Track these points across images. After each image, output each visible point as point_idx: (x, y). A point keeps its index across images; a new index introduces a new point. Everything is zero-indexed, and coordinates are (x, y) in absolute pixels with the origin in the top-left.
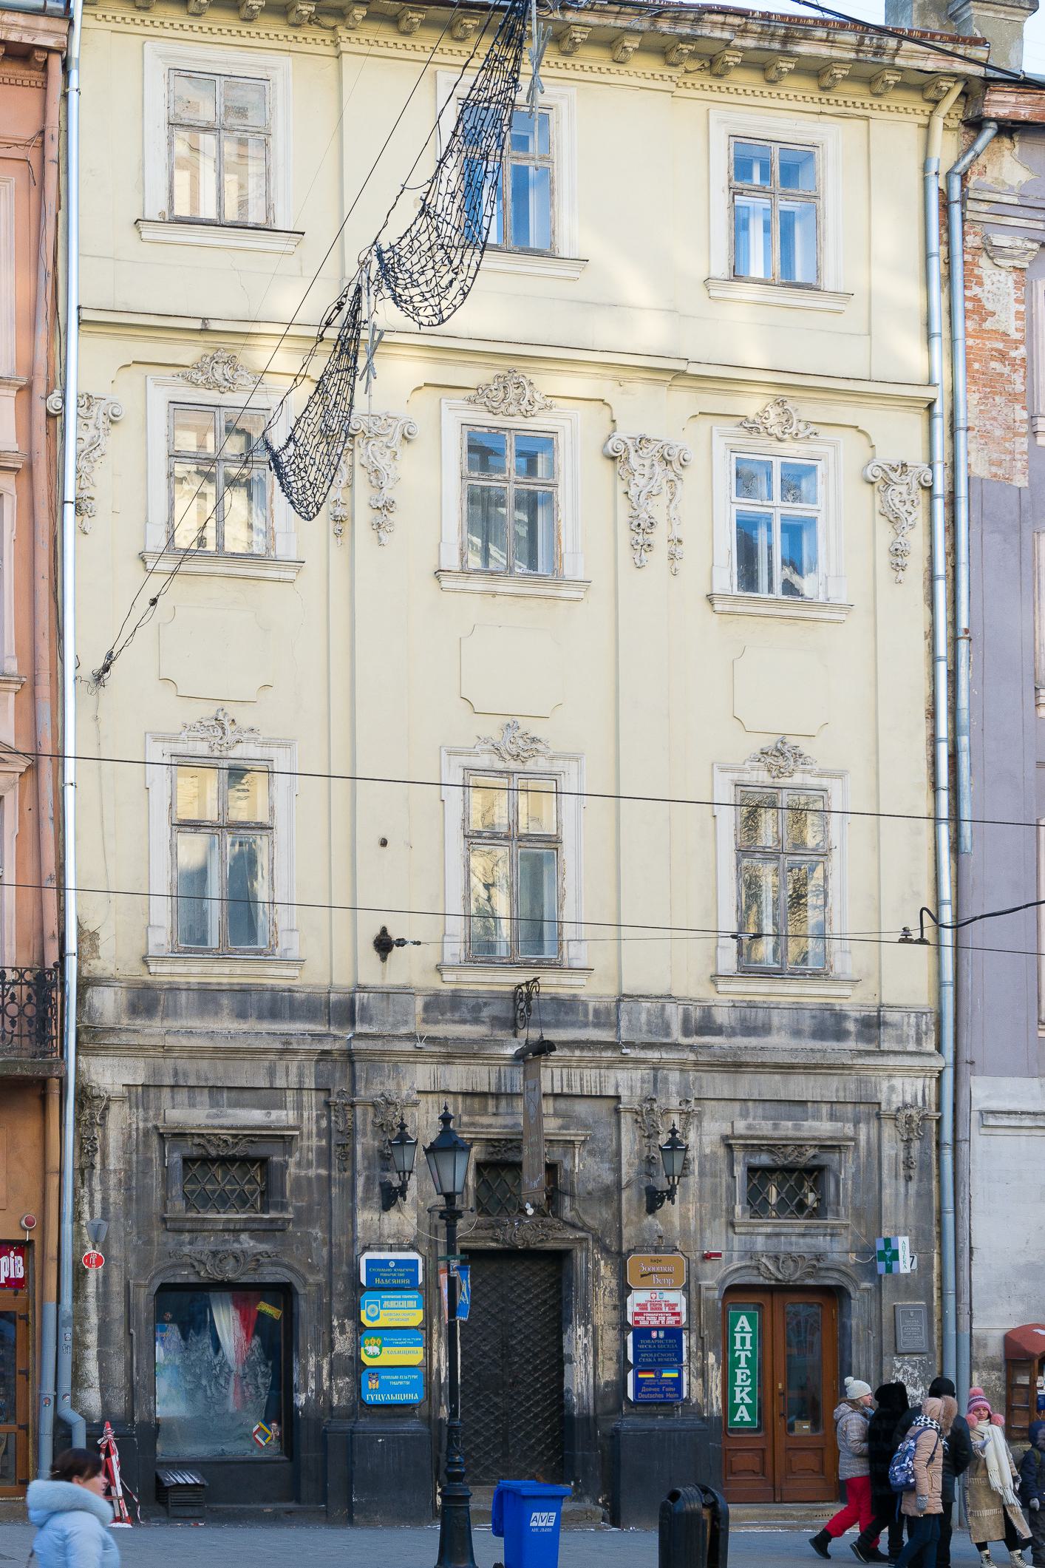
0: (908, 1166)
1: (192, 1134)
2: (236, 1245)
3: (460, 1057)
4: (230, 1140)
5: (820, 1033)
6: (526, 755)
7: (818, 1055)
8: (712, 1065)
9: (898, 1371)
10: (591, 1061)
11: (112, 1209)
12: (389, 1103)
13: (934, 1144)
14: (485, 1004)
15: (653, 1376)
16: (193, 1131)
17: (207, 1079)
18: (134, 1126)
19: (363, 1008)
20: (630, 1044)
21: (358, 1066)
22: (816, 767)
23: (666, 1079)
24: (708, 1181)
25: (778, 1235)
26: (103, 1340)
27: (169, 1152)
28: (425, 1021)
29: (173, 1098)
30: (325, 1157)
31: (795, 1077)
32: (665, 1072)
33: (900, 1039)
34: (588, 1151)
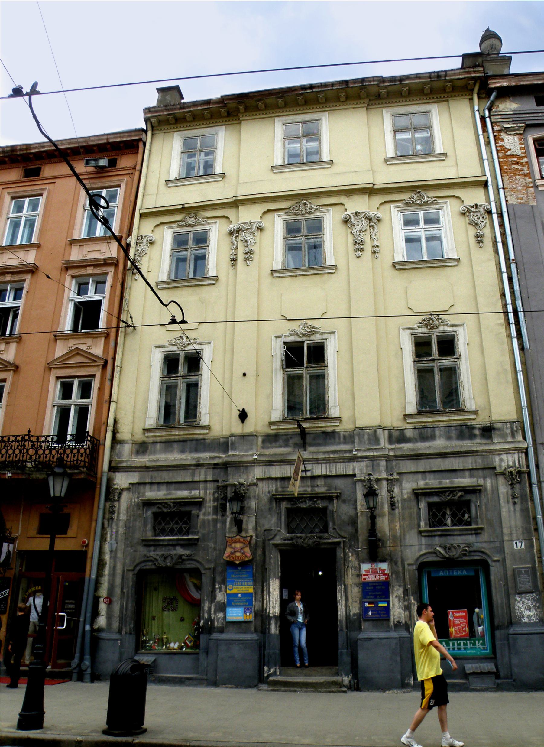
0: (514, 497)
4: (172, 505)
9: (519, 602)
10: (340, 459)
11: (119, 536)
12: (241, 484)
13: (527, 485)
14: (291, 438)
17: (164, 479)
19: (232, 444)
21: (229, 469)
22: (450, 323)
23: (378, 465)
27: (146, 511)
28: (263, 448)
29: (151, 488)
30: (215, 509)
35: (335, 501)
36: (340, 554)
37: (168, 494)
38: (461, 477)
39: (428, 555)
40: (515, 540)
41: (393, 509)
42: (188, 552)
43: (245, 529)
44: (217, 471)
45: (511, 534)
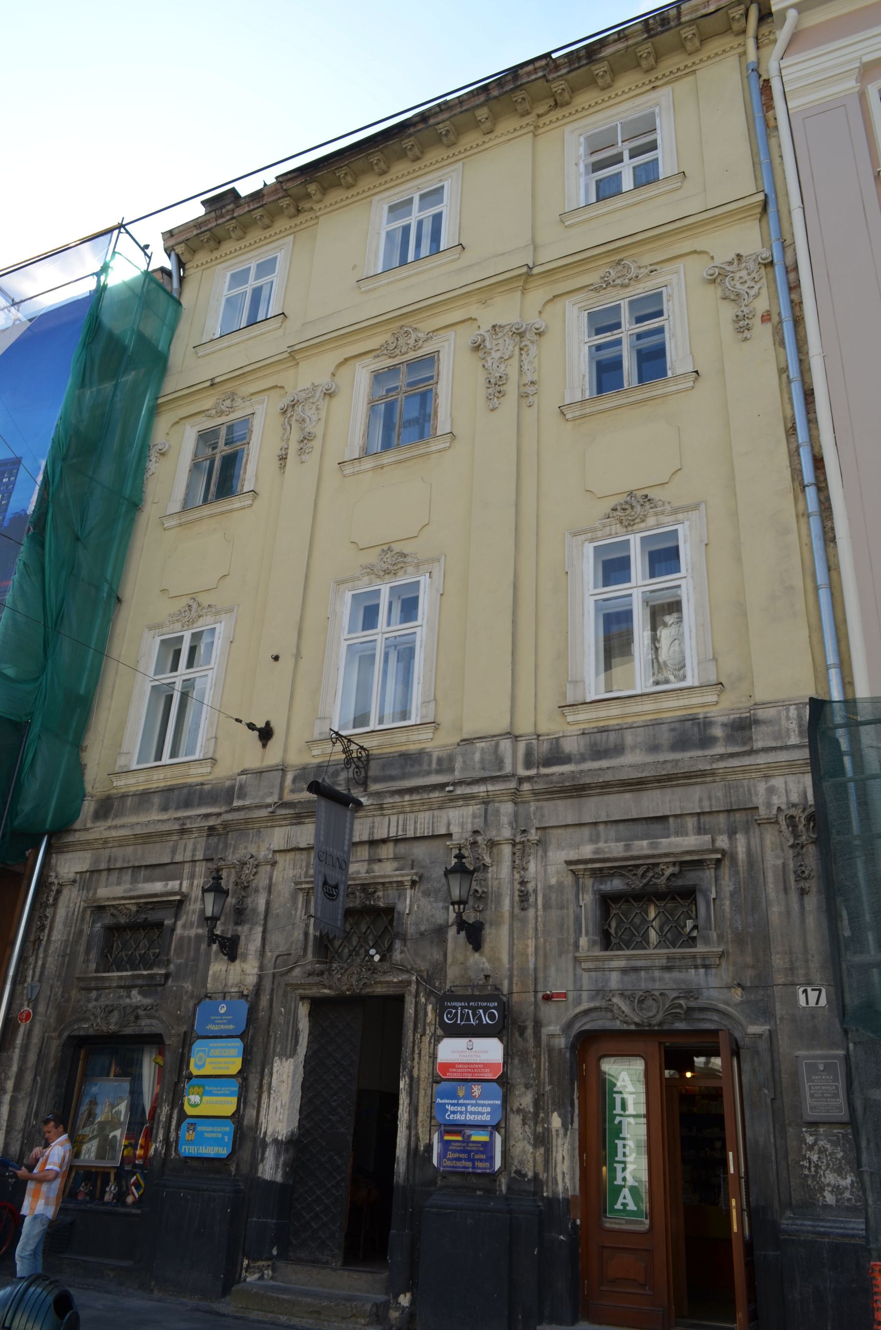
0: (800, 876)
1: (109, 906)
2: (128, 1001)
3: (308, 817)
5: (681, 743)
6: (395, 568)
7: (669, 766)
8: (552, 792)
9: (811, 1148)
11: (46, 973)
15: (460, 1138)
16: (107, 903)
17: (129, 861)
18: (78, 905)
20: (460, 783)
23: (497, 812)
24: (554, 914)
25: (636, 969)
26: (17, 1088)
28: (292, 791)
29: (107, 879)
31: (649, 792)
32: (496, 805)
33: (778, 736)
34: (423, 892)
35: (408, 892)
36: (410, 1010)
37: (131, 890)
38: (677, 834)
39: (594, 1015)
40: (801, 985)
41: (523, 909)
42: (148, 1001)
43: (242, 954)
44: (214, 840)
45: (792, 969)
